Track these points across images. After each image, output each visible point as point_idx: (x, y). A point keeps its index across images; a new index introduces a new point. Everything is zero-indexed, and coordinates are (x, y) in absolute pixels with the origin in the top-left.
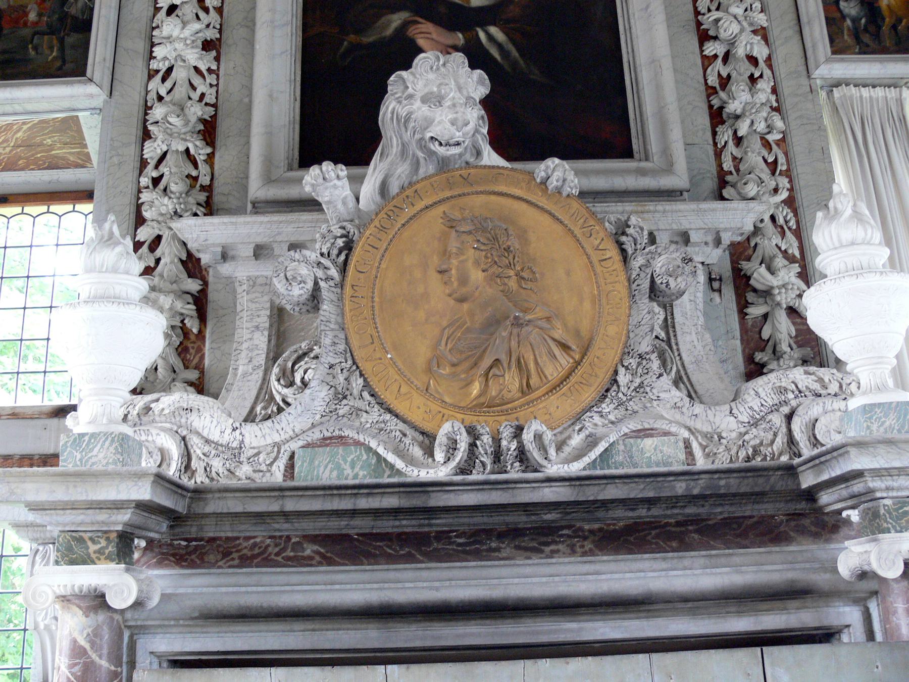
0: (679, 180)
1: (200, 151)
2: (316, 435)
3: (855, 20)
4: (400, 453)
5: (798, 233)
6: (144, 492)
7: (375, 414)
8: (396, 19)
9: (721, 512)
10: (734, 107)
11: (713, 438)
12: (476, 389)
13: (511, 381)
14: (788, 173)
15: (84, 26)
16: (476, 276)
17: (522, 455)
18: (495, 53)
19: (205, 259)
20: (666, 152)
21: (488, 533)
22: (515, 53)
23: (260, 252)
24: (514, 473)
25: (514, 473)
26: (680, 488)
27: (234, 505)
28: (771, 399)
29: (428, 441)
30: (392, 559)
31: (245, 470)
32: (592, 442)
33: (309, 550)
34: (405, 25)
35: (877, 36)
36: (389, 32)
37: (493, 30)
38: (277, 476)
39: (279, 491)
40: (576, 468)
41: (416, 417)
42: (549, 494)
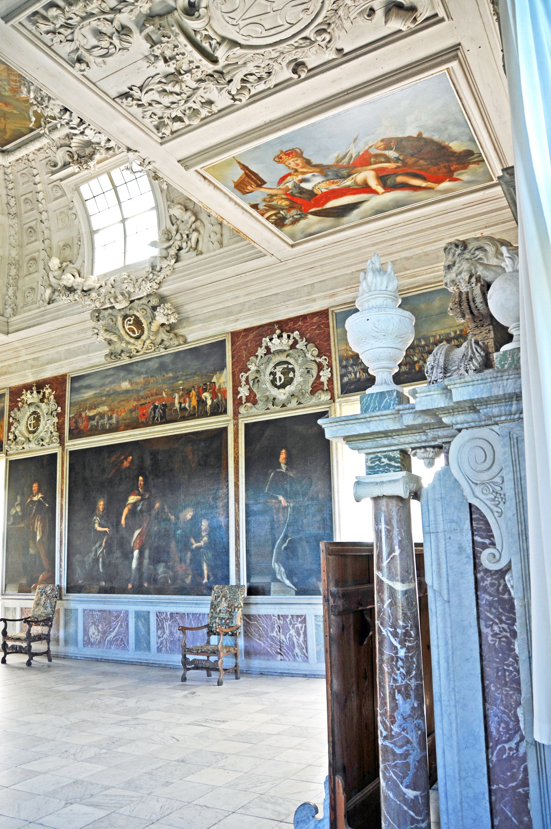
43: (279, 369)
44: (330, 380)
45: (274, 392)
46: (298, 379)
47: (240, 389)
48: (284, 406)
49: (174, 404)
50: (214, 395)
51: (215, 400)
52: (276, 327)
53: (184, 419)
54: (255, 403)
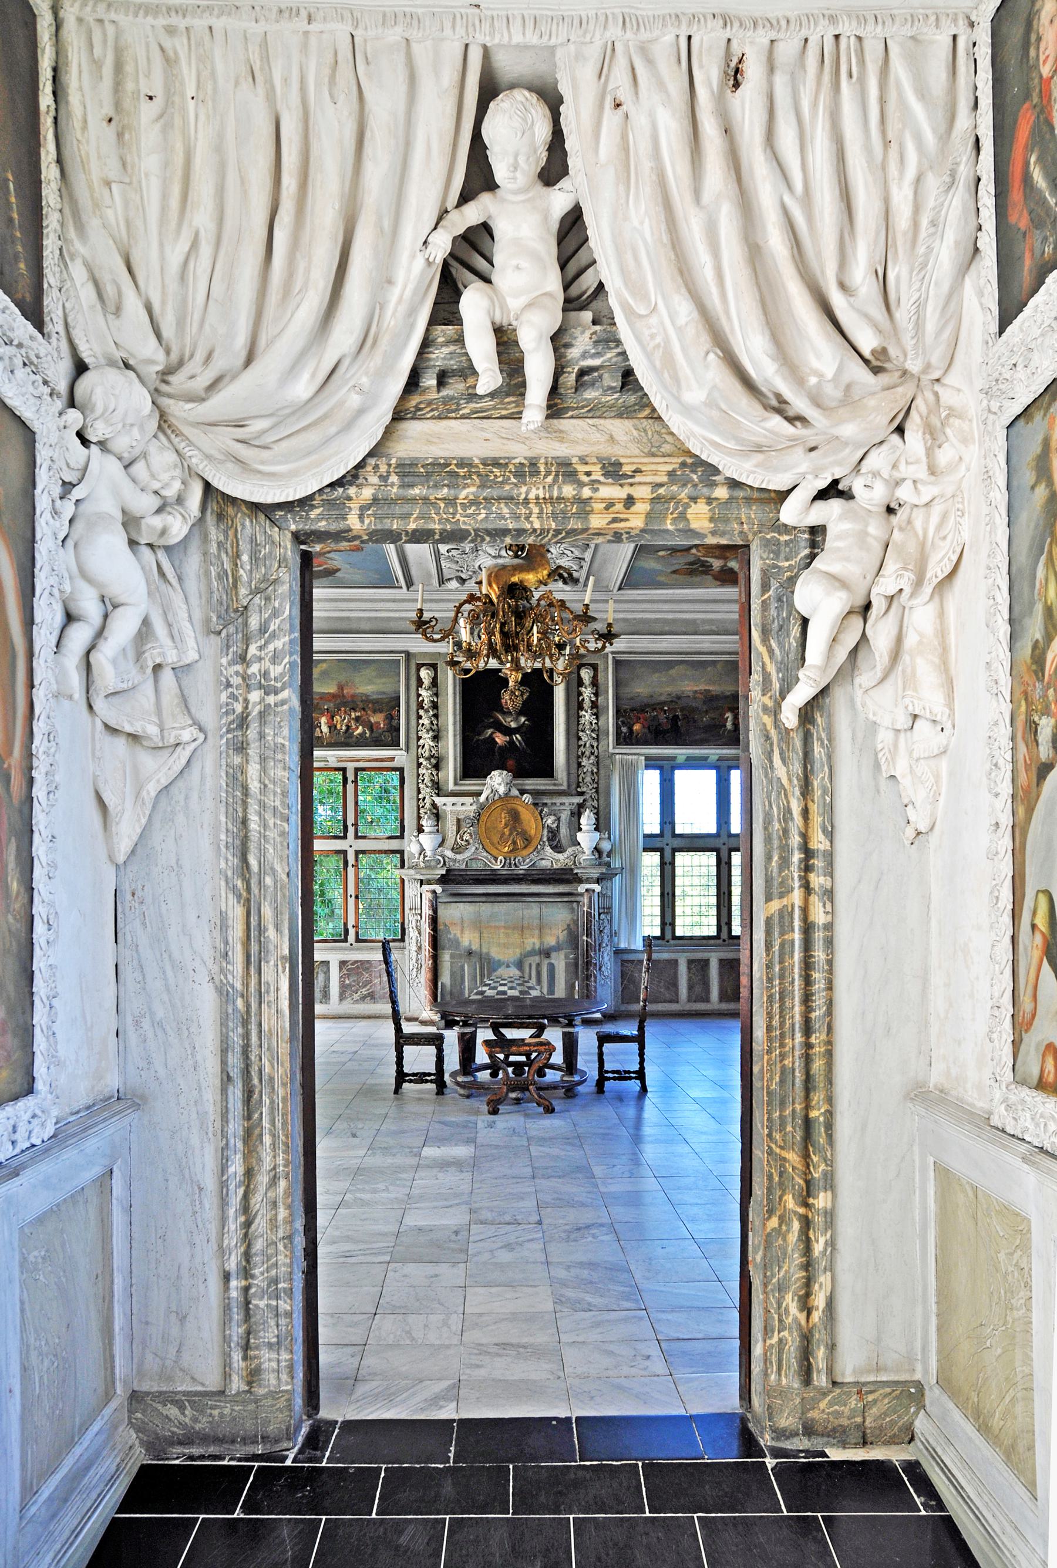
0: (564, 787)
1: (434, 773)
8: (490, 731)
9: (558, 877)
11: (558, 861)
29: (496, 859)
35: (631, 739)
38: (463, 867)
42: (521, 872)
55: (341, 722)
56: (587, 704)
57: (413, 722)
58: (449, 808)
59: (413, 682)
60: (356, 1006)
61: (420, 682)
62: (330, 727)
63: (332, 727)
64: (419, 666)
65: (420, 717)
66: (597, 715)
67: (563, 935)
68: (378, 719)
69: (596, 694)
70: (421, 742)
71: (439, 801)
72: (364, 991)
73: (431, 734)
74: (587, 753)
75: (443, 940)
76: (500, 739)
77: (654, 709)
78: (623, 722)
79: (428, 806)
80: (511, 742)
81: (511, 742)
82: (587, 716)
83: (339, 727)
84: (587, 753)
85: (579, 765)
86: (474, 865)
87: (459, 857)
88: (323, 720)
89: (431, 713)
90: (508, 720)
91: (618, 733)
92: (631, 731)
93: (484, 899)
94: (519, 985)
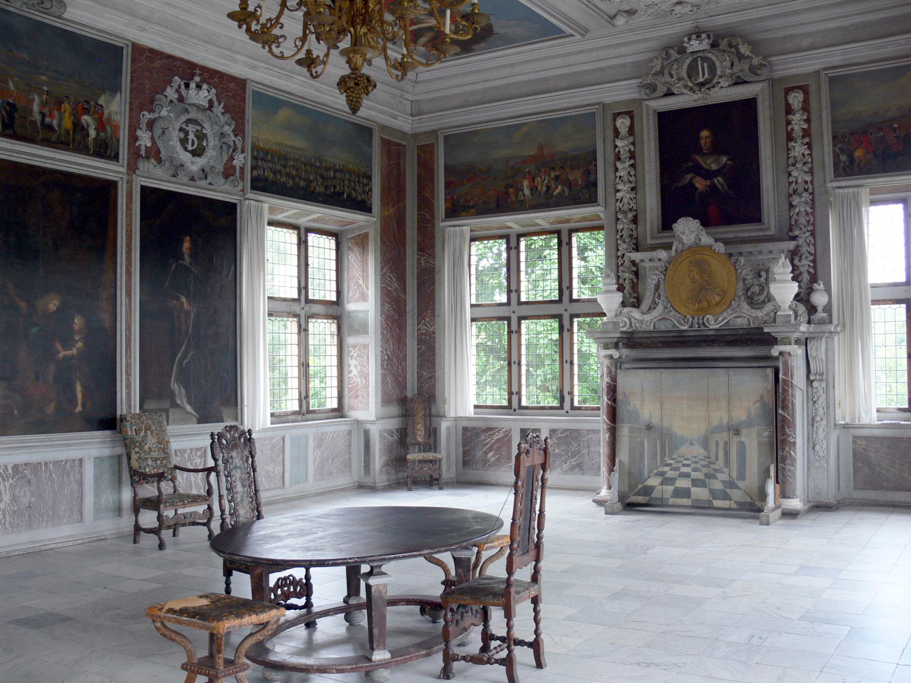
0: (772, 231)
1: (632, 226)
2: (660, 318)
3: (844, 163)
4: (679, 322)
5: (814, 245)
6: (618, 335)
7: (673, 313)
8: (689, 177)
10: (794, 203)
12: (696, 306)
13: (705, 304)
14: (813, 225)
15: (595, 185)
16: (697, 277)
17: (704, 324)
18: (720, 187)
19: (637, 262)
20: (769, 223)
21: (700, 341)
22: (726, 187)
23: (650, 260)
24: (703, 328)
25: (703, 328)
26: (741, 332)
27: (640, 335)
28: (772, 308)
30: (677, 347)
31: (644, 326)
32: (725, 318)
33: (659, 345)
34: (692, 178)
36: (687, 182)
37: (719, 178)
39: (651, 332)
40: (717, 327)
41: (683, 313)
42: (710, 333)
43: (191, 128)
44: (242, 169)
45: (185, 157)
46: (210, 153)
47: (139, 133)
48: (192, 179)
49: (31, 110)
50: (101, 126)
51: (102, 134)
52: (198, 72)
53: (47, 143)
54: (159, 161)
55: (542, 183)
56: (797, 132)
57: (611, 176)
58: (647, 264)
59: (610, 133)
60: (565, 476)
61: (617, 133)
62: (531, 190)
63: (533, 189)
64: (616, 116)
65: (617, 170)
66: (809, 145)
67: (755, 408)
68: (576, 176)
69: (808, 121)
70: (619, 195)
71: (636, 256)
72: (573, 461)
73: (628, 187)
74: (801, 189)
75: (621, 412)
76: (700, 184)
77: (880, 129)
78: (841, 149)
79: (627, 263)
80: (713, 187)
81: (713, 187)
82: (799, 149)
83: (539, 188)
84: (801, 189)
85: (791, 206)
86: (663, 327)
87: (647, 318)
88: (526, 183)
89: (628, 163)
90: (709, 161)
91: (836, 164)
92: (851, 159)
93: (671, 364)
94: (704, 466)
